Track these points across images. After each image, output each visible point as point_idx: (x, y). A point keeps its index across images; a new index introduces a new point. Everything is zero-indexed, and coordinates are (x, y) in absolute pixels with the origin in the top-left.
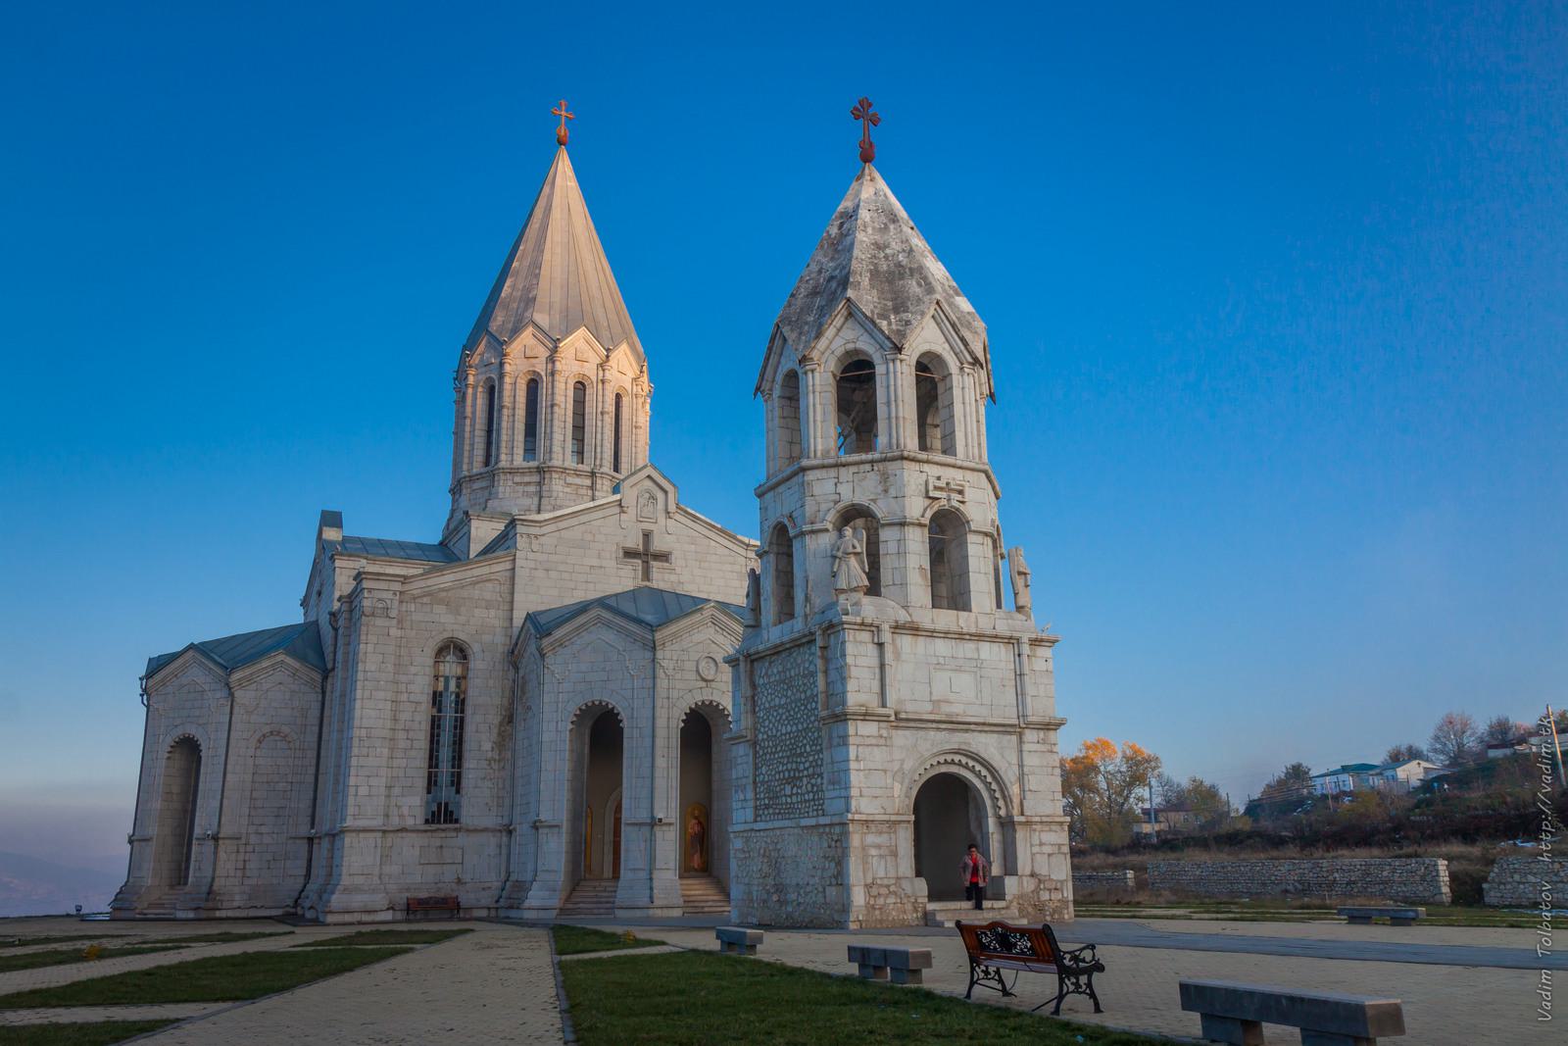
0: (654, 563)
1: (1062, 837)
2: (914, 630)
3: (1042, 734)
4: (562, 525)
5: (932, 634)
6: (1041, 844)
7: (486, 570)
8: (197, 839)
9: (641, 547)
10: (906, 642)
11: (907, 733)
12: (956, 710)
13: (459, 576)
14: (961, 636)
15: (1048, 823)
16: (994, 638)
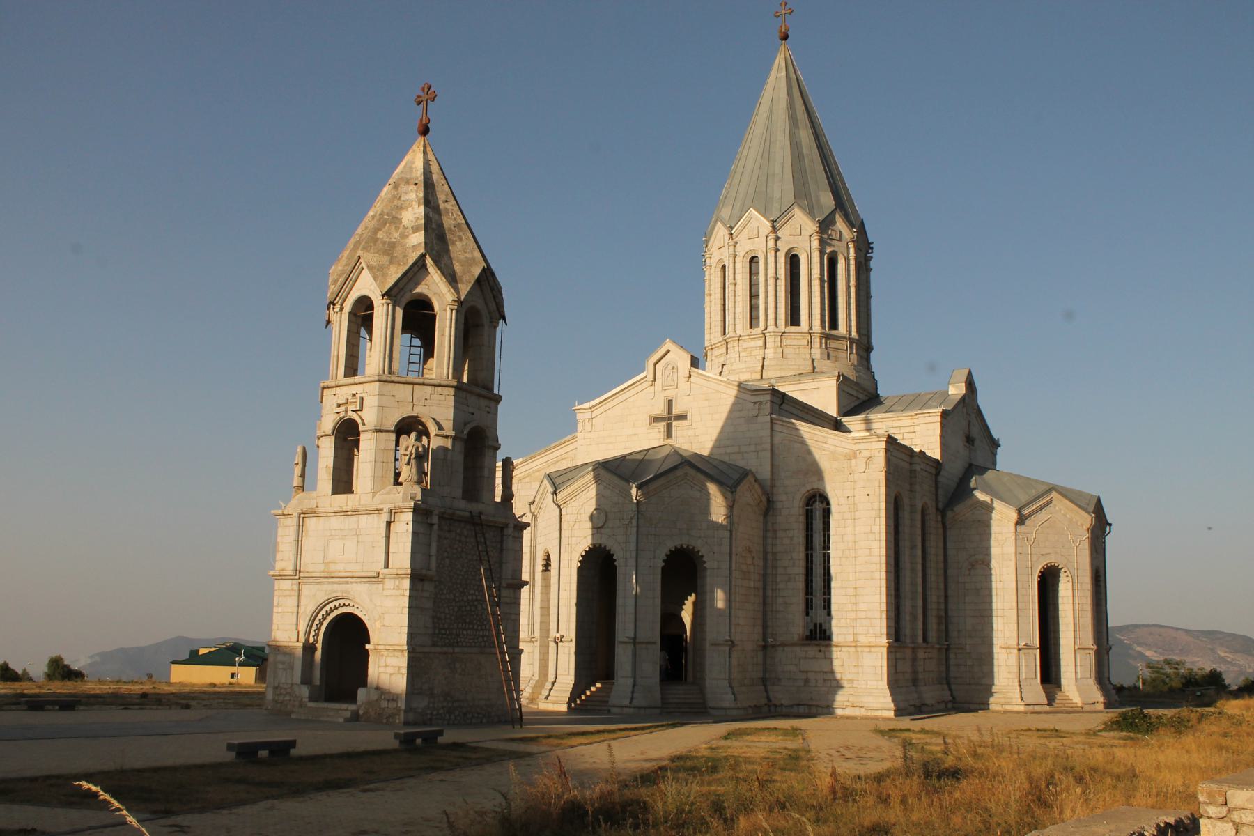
0: (675, 424)
1: (403, 662)
2: (315, 513)
3: (397, 582)
4: (606, 407)
5: (326, 514)
6: (386, 666)
7: (562, 451)
8: (654, 643)
9: (665, 414)
10: (311, 523)
11: (311, 586)
12: (340, 568)
13: (546, 459)
14: (346, 513)
15: (392, 650)
16: (367, 511)
